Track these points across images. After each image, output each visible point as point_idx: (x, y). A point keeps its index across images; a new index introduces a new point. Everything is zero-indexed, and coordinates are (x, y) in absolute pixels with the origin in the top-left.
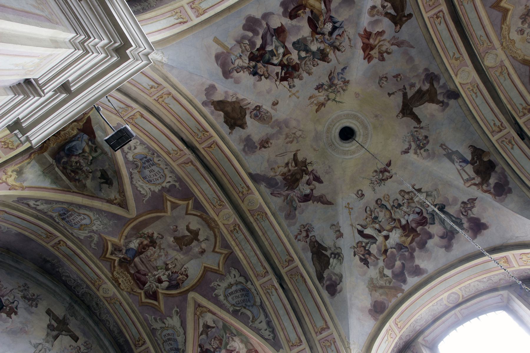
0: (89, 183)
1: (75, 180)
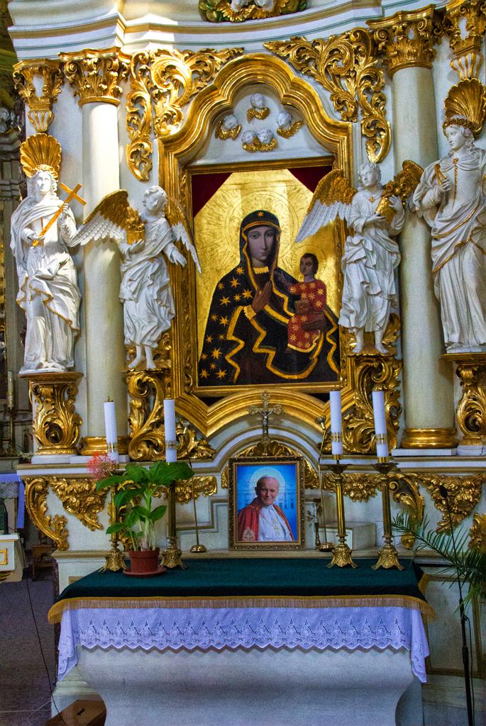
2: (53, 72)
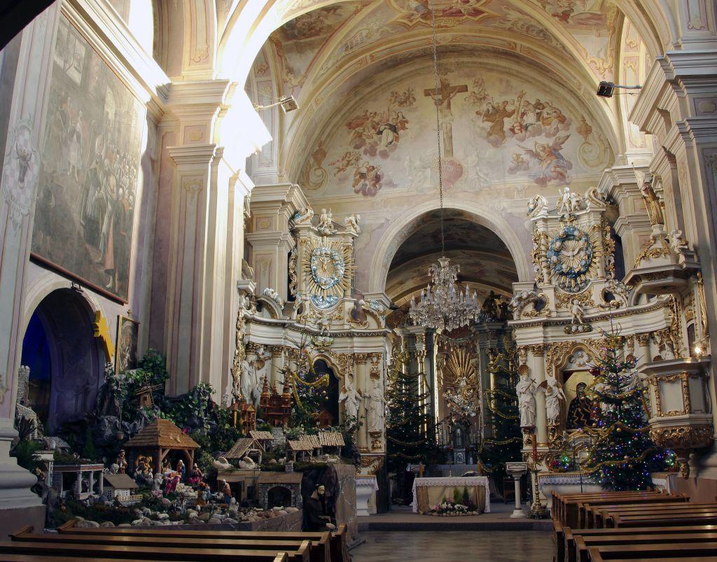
0: (328, 22)
1: (320, 31)
2: (526, 348)
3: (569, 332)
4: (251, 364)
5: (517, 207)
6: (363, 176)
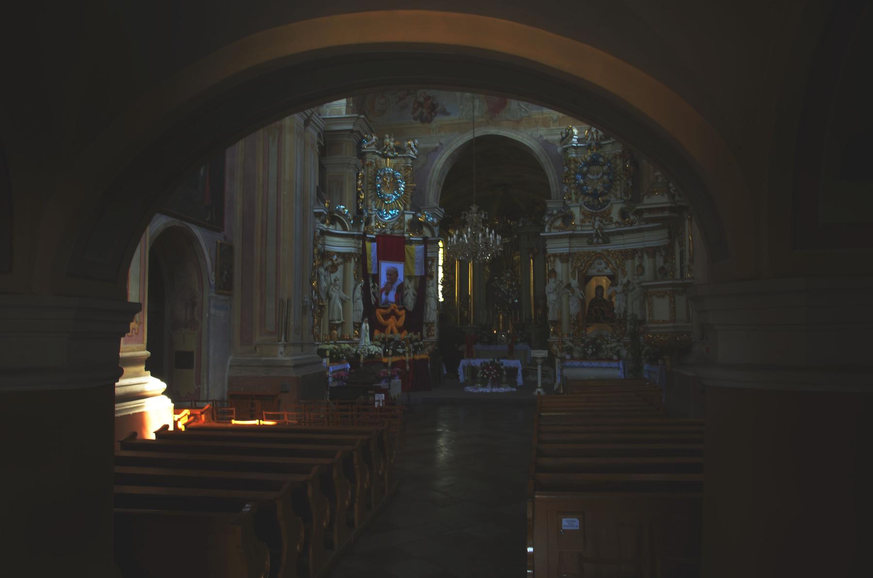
2: (555, 255)
3: (590, 243)
4: (326, 269)
5: (552, 135)
6: (421, 105)
